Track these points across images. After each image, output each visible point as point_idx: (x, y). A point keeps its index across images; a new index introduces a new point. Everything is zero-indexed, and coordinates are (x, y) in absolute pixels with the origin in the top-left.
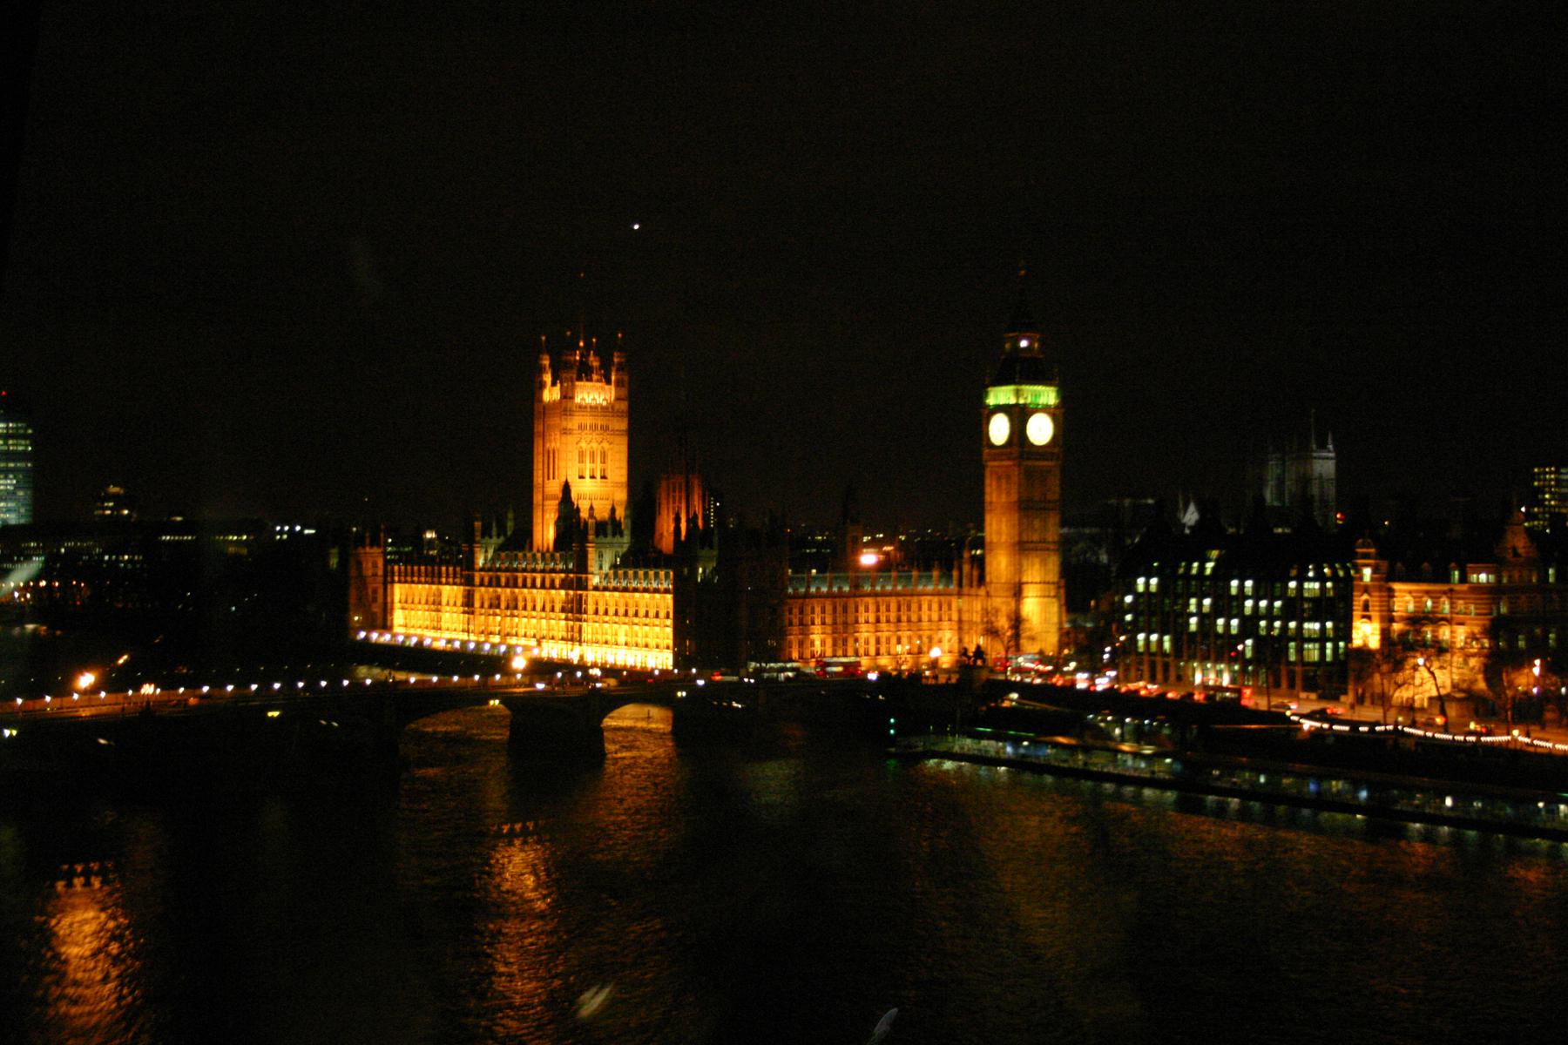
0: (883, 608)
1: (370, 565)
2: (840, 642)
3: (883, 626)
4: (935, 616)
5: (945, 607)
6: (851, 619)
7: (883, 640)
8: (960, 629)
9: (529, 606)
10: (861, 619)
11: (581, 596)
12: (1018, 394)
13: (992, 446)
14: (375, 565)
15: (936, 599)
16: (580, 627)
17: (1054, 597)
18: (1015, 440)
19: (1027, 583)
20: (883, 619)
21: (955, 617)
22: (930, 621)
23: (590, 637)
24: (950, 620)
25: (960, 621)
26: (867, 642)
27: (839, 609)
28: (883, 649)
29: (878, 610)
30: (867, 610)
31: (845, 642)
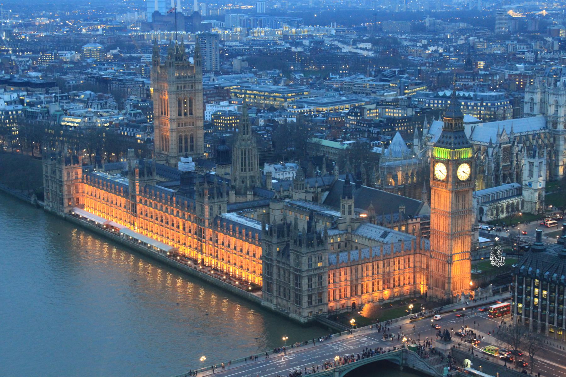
0: (375, 267)
1: (74, 173)
2: (354, 288)
3: (376, 276)
4: (402, 267)
5: (407, 261)
6: (360, 275)
7: (376, 283)
8: (415, 272)
9: (170, 223)
10: (365, 275)
11: (201, 229)
12: (453, 154)
13: (437, 180)
14: (76, 173)
15: (402, 258)
16: (201, 245)
17: (468, 259)
18: (450, 179)
19: (454, 254)
20: (375, 272)
21: (412, 265)
22: (399, 269)
23: (207, 252)
24: (409, 267)
25: (415, 267)
26: (368, 286)
27: (354, 271)
28: (375, 288)
29: (373, 268)
30: (367, 269)
31: (356, 287)
